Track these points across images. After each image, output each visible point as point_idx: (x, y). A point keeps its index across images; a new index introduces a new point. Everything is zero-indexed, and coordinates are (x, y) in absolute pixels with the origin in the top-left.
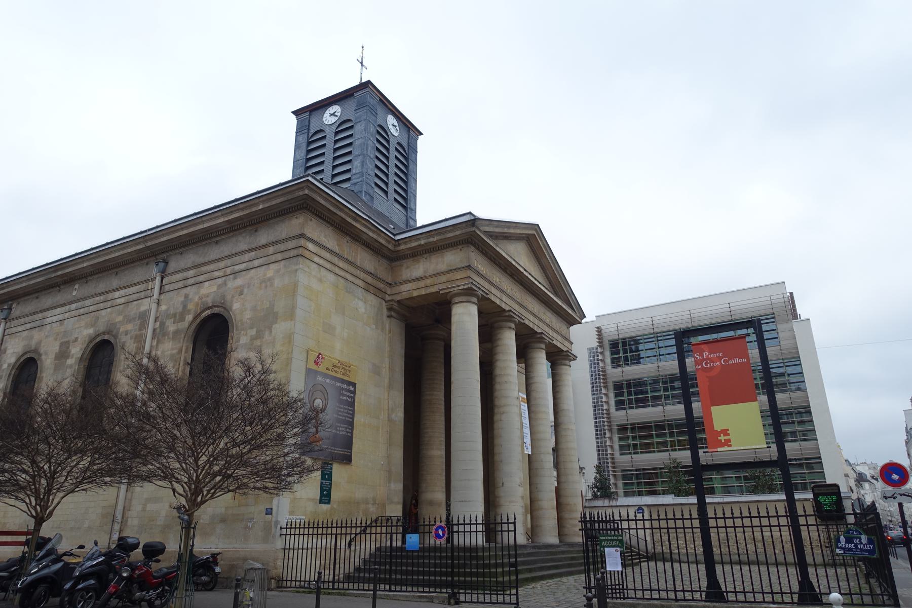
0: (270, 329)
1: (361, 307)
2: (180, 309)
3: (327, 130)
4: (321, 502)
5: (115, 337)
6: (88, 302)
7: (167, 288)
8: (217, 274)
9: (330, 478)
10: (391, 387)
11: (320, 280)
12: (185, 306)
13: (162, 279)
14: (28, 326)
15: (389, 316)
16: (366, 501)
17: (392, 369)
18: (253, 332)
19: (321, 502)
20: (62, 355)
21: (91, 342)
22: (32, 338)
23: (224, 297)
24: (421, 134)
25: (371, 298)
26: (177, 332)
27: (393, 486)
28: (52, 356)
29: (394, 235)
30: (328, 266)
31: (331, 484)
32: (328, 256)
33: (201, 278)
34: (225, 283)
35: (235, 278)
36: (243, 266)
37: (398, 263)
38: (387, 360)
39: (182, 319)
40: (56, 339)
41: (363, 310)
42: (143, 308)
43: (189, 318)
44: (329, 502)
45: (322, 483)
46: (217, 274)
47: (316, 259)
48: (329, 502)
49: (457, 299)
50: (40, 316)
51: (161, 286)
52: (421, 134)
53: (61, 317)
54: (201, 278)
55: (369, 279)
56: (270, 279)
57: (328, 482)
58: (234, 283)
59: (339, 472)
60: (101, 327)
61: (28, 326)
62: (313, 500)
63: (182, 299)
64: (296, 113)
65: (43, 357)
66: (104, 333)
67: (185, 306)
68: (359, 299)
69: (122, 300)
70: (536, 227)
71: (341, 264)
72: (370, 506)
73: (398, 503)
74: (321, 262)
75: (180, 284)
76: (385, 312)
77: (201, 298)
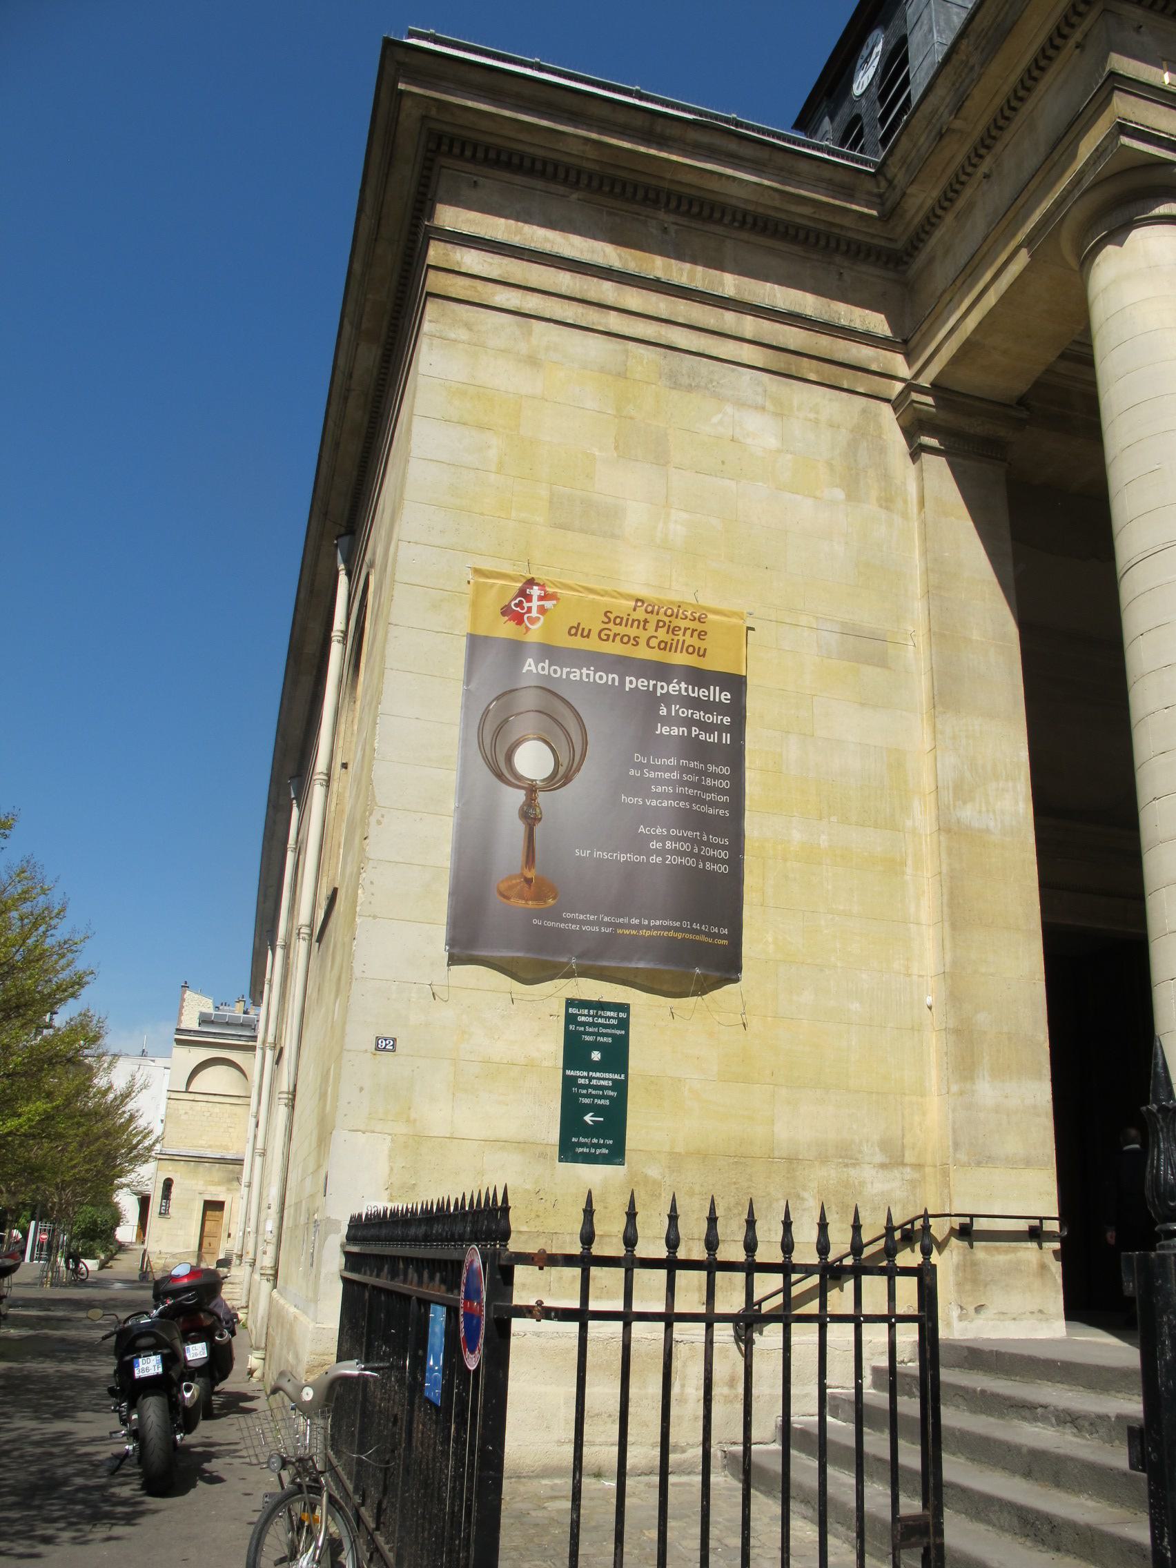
4: (568, 1152)
9: (617, 1056)
10: (946, 695)
11: (532, 361)
16: (847, 1155)
19: (568, 1152)
27: (986, 1090)
31: (621, 1088)
32: (565, 281)
38: (918, 608)
41: (772, 442)
44: (616, 1154)
45: (568, 1083)
48: (616, 1154)
57: (604, 1079)
59: (666, 1037)
62: (522, 1145)
68: (740, 404)
71: (634, 299)
72: (867, 1173)
74: (532, 303)
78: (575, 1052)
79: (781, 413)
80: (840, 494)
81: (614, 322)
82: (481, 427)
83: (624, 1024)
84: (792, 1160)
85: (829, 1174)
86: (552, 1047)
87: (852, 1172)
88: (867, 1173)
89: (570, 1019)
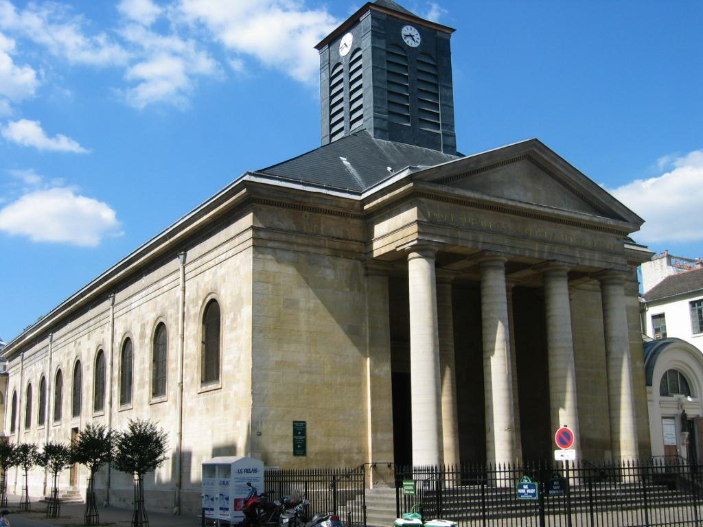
0: (240, 311)
1: (330, 274)
2: (195, 296)
3: (344, 63)
5: (166, 319)
6: (150, 290)
7: (187, 277)
8: (212, 263)
9: (304, 433)
12: (197, 292)
13: (184, 268)
14: (124, 310)
15: (367, 275)
17: (373, 328)
18: (232, 315)
19: (295, 454)
20: (142, 336)
21: (155, 324)
22: (126, 321)
23: (216, 284)
24: (453, 30)
25: (343, 263)
26: (195, 314)
28: (138, 336)
29: (360, 194)
30: (284, 246)
32: (283, 237)
33: (204, 268)
34: (216, 272)
35: (221, 267)
36: (223, 257)
37: (371, 220)
39: (197, 305)
40: (138, 322)
41: (332, 277)
42: (177, 295)
43: (200, 302)
45: (294, 439)
46: (212, 263)
47: (270, 244)
49: (411, 256)
50: (128, 302)
51: (184, 275)
52: (453, 30)
53: (139, 303)
54: (204, 268)
55: (337, 245)
56: (238, 268)
57: (301, 438)
58: (221, 270)
60: (159, 313)
61: (124, 310)
62: (287, 453)
63: (195, 286)
64: (316, 47)
65: (134, 337)
66: (160, 317)
67: (197, 292)
68: (325, 267)
69: (166, 288)
70: (535, 142)
72: (354, 455)
73: (388, 451)
74: (276, 245)
75: (193, 274)
76: (362, 272)
77: (205, 286)
78: (295, 433)
79: (335, 269)
80: (348, 289)
81: (295, 247)
82: (267, 283)
83: (305, 426)
84: (339, 453)
85: (345, 456)
86: (291, 432)
87: (351, 455)
88: (354, 455)
89: (294, 425)
